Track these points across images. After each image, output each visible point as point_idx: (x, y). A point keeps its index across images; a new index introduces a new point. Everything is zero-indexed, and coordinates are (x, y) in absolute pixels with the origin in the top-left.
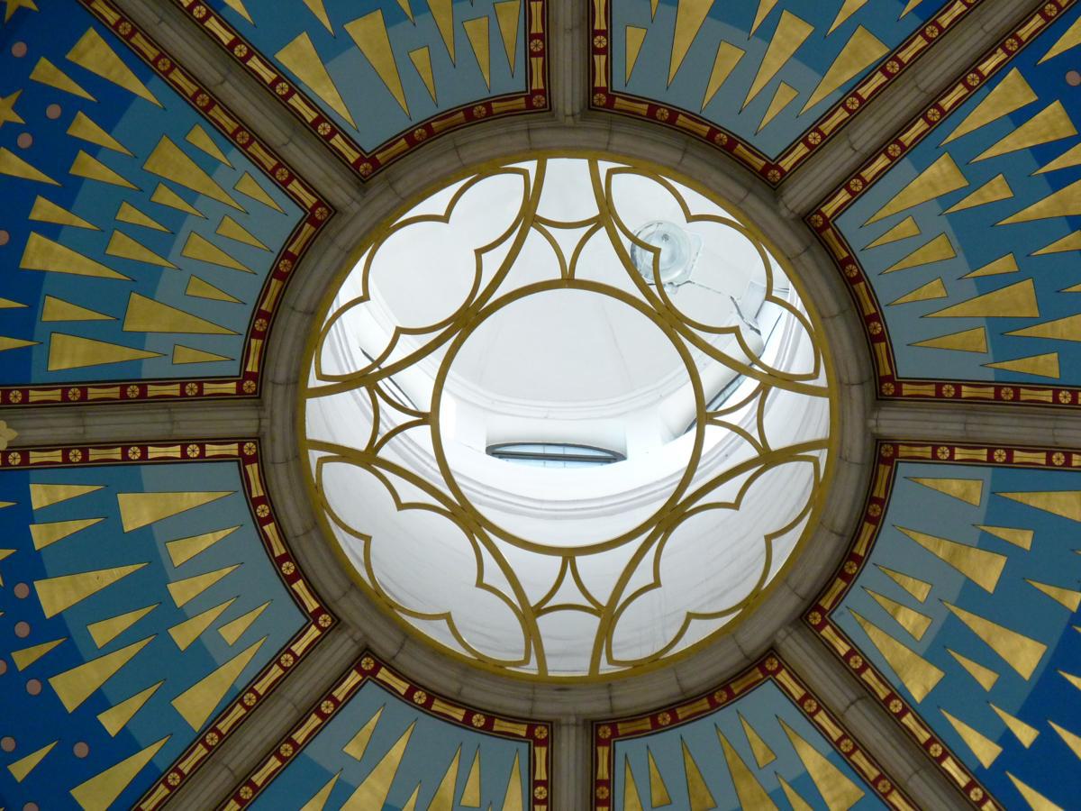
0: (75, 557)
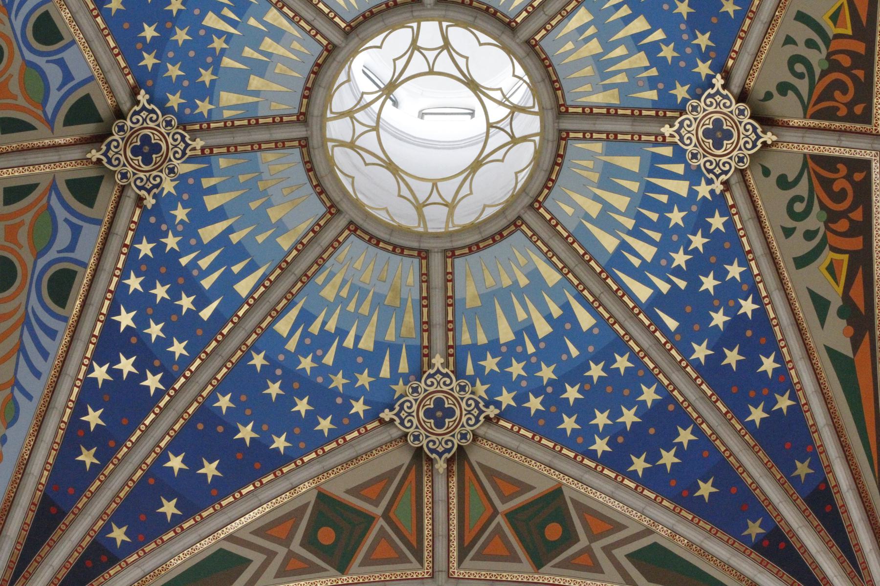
0: (491, 327)
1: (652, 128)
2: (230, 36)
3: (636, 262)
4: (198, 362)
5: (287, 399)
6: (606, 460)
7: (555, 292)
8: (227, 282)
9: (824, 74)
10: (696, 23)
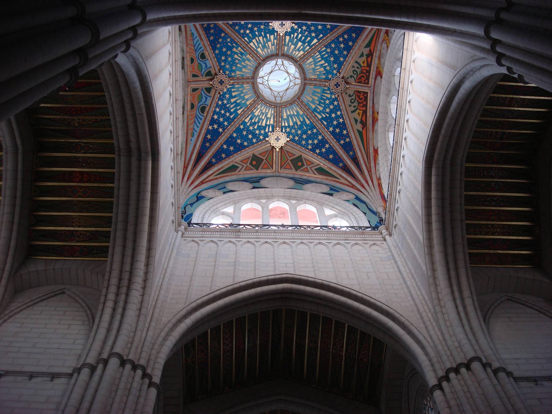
0: (288, 123)
1: (324, 83)
2: (239, 60)
3: (319, 111)
4: (230, 126)
5: (247, 135)
6: (311, 150)
7: (302, 116)
8: (236, 110)
9: (360, 74)
10: (334, 62)
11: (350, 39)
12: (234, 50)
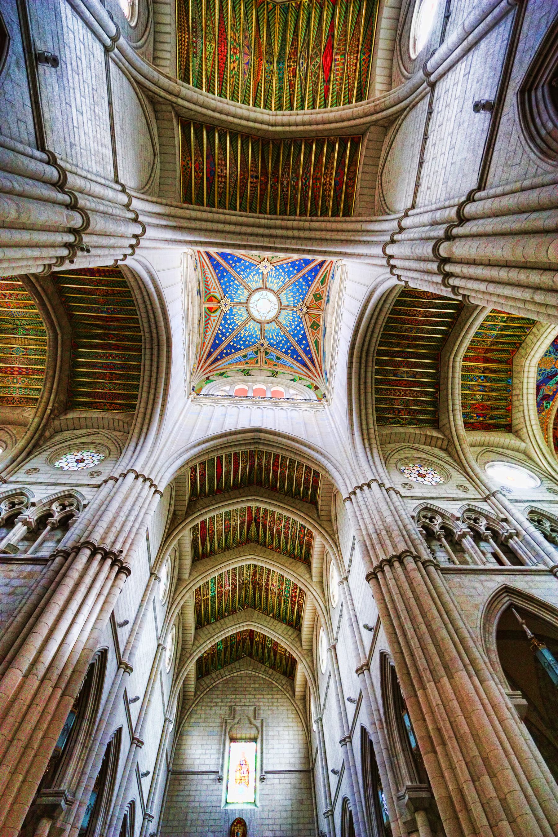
5: (297, 330)
8: (281, 336)
10: (250, 269)
11: (232, 259)
12: (242, 336)
